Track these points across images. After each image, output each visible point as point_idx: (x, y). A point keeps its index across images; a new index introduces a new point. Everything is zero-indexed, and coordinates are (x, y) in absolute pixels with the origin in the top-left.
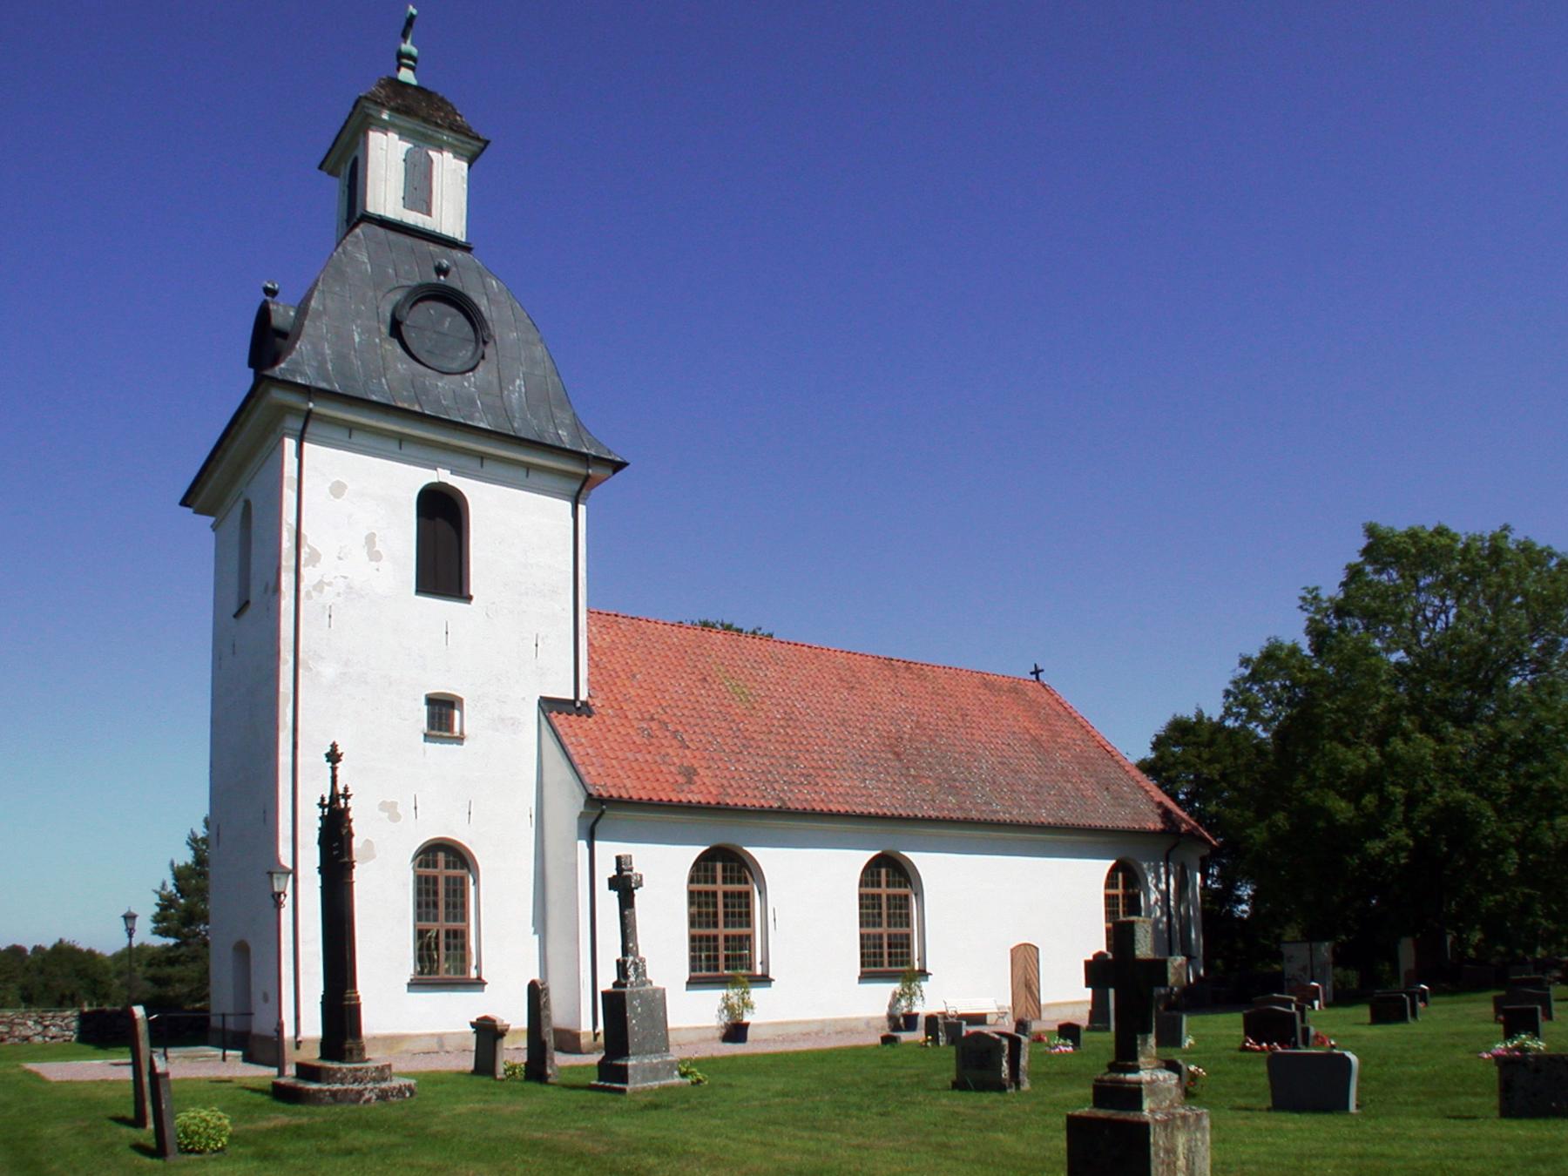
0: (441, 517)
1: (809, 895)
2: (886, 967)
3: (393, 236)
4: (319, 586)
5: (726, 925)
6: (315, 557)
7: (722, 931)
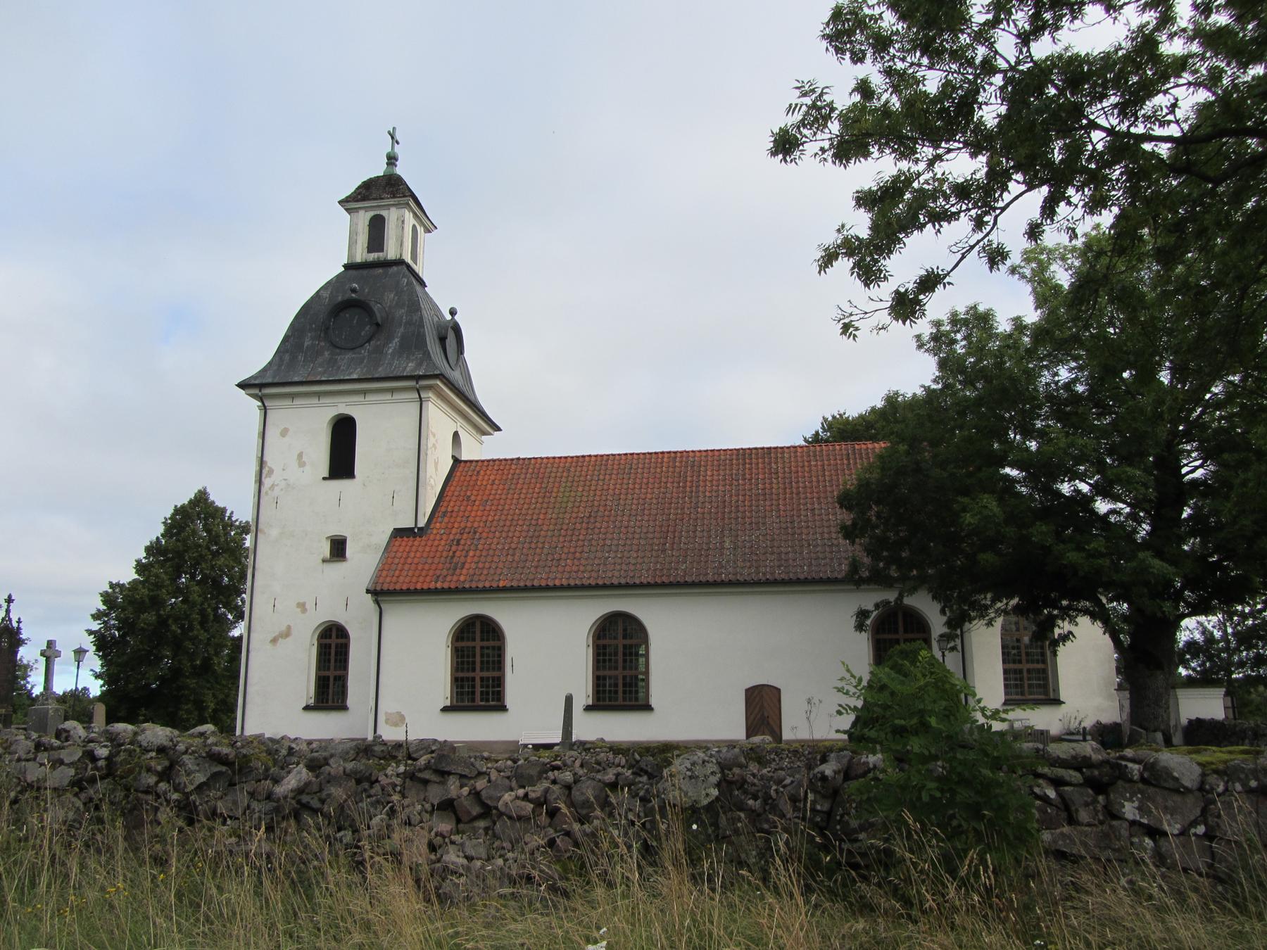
0: (343, 435)
2: (620, 702)
3: (365, 272)
5: (482, 670)
6: (271, 471)
7: (478, 674)
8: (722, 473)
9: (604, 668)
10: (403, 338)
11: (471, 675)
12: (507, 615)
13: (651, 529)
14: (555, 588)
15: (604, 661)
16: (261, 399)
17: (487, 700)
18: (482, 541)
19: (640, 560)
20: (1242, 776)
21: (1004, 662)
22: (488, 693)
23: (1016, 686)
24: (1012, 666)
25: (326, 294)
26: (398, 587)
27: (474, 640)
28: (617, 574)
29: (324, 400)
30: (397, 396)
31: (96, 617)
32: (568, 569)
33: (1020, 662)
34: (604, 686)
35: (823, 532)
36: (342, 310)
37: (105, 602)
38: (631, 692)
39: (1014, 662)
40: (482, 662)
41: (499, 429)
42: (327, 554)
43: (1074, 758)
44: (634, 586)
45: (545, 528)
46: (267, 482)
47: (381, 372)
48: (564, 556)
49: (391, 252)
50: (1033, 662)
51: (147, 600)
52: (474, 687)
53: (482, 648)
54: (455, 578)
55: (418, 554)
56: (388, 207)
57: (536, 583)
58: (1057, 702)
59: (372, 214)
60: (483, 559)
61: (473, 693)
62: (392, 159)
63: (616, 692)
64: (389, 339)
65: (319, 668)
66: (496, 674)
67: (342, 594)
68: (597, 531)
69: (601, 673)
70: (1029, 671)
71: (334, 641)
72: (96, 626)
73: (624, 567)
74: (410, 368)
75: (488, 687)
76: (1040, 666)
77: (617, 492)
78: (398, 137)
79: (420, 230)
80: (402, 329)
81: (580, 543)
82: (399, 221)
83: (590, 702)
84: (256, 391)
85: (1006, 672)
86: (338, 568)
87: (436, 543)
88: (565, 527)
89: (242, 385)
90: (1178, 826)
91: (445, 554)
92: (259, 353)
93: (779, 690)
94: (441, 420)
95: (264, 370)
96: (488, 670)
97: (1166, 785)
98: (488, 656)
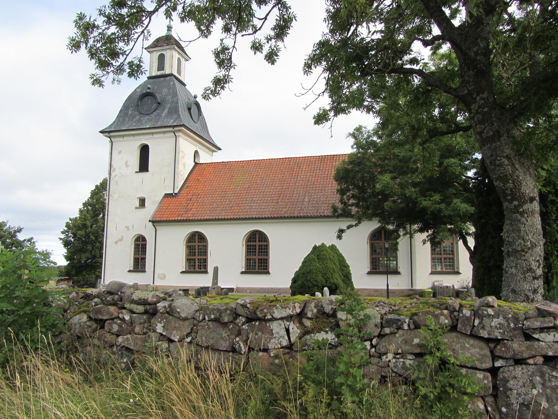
1: (227, 246)
2: (257, 270)
3: (156, 80)
5: (198, 255)
6: (115, 169)
8: (310, 167)
9: (250, 255)
10: (170, 109)
11: (194, 257)
12: (208, 231)
13: (274, 193)
14: (228, 219)
15: (262, 252)
16: (110, 138)
17: (201, 269)
18: (201, 199)
19: (266, 207)
20: (208, 312)
21: (432, 254)
22: (201, 266)
23: (450, 265)
24: (437, 256)
25: (139, 90)
26: (162, 219)
27: (195, 242)
28: (255, 213)
29: (136, 138)
30: (166, 135)
31: (63, 233)
32: (235, 211)
33: (441, 254)
34: (250, 263)
35: (329, 193)
36: (144, 97)
37: (66, 226)
38: (261, 266)
39: (438, 254)
40: (198, 252)
41: (220, 149)
43: (140, 299)
44: (262, 218)
45: (228, 193)
47: (159, 124)
48: (234, 205)
49: (167, 71)
50: (447, 254)
51: (81, 225)
52: (195, 263)
53: (198, 246)
54: (186, 215)
55: (173, 205)
57: (220, 217)
58: (458, 273)
59: (159, 53)
60: (200, 207)
61: (195, 265)
62: (169, 28)
63: (255, 266)
64: (164, 110)
65: (135, 254)
66: (204, 257)
67: (140, 221)
68: (250, 194)
69: (249, 257)
70: (445, 258)
71: (140, 243)
72: (63, 236)
73: (259, 210)
74: (171, 122)
75: (201, 263)
76: (451, 256)
77: (262, 176)
79: (182, 60)
80: (169, 105)
81: (242, 199)
82: (171, 56)
83: (244, 270)
84: (107, 134)
86: (142, 211)
87: (182, 200)
88: (237, 192)
89: (102, 132)
90: (178, 337)
91: (184, 204)
94: (187, 147)
95: (112, 125)
96: (201, 255)
97: (175, 315)
98: (201, 249)
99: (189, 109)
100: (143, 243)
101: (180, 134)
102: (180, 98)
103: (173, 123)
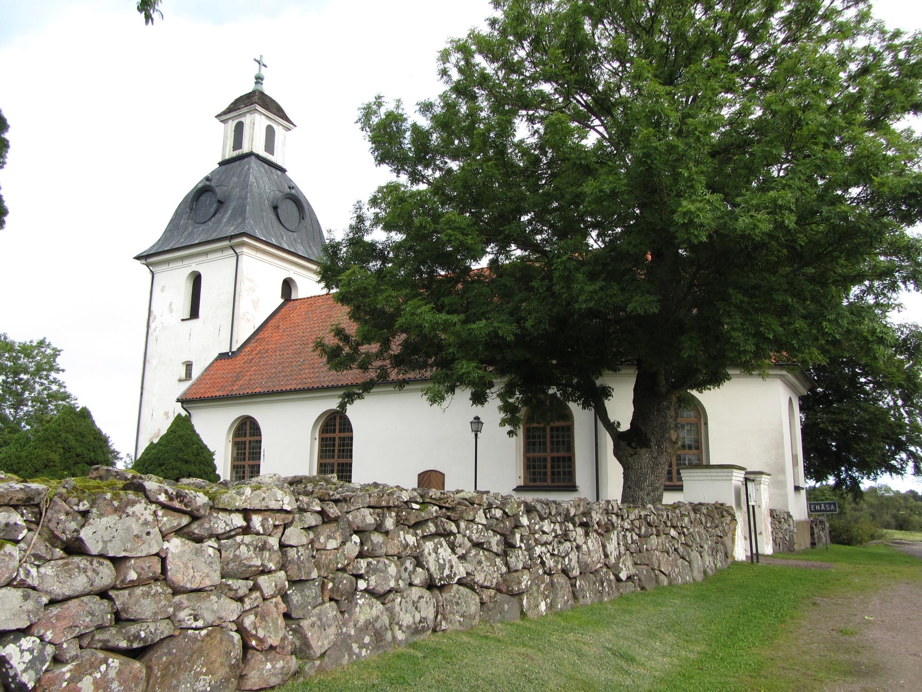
4: (155, 330)
6: (155, 318)
10: (233, 210)
12: (262, 414)
29: (186, 262)
42: (183, 376)
46: (152, 325)
47: (214, 236)
49: (246, 149)
56: (244, 114)
59: (236, 121)
62: (259, 79)
64: (226, 212)
74: (231, 230)
78: (264, 61)
84: (144, 261)
85: (351, 457)
89: (138, 258)
92: (151, 233)
93: (443, 475)
95: (154, 246)
99: (275, 208)
100: (252, 438)
101: (245, 250)
102: (255, 190)
103: (233, 231)
